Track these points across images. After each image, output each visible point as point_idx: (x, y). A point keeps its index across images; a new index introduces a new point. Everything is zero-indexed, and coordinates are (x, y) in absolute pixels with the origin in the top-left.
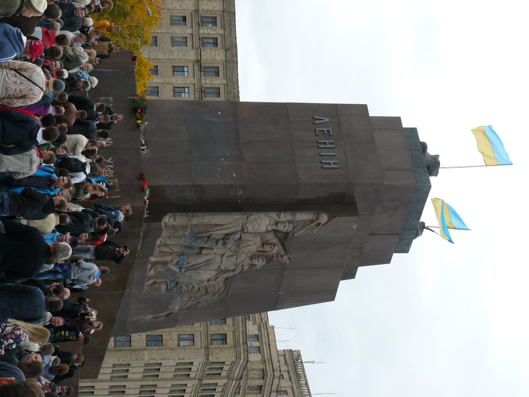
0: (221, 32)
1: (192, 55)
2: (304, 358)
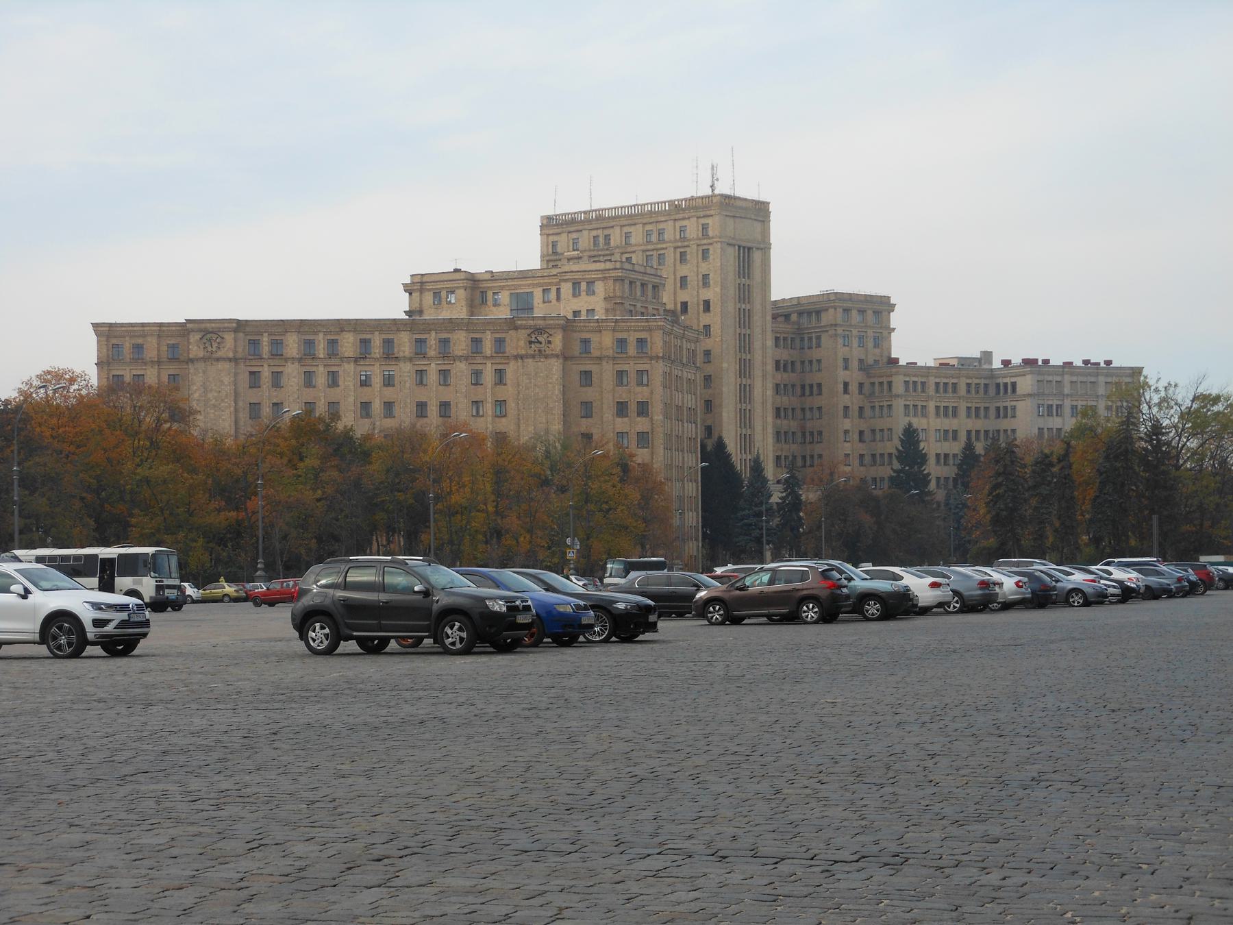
0: (321, 335)
1: (350, 367)
2: (550, 213)
